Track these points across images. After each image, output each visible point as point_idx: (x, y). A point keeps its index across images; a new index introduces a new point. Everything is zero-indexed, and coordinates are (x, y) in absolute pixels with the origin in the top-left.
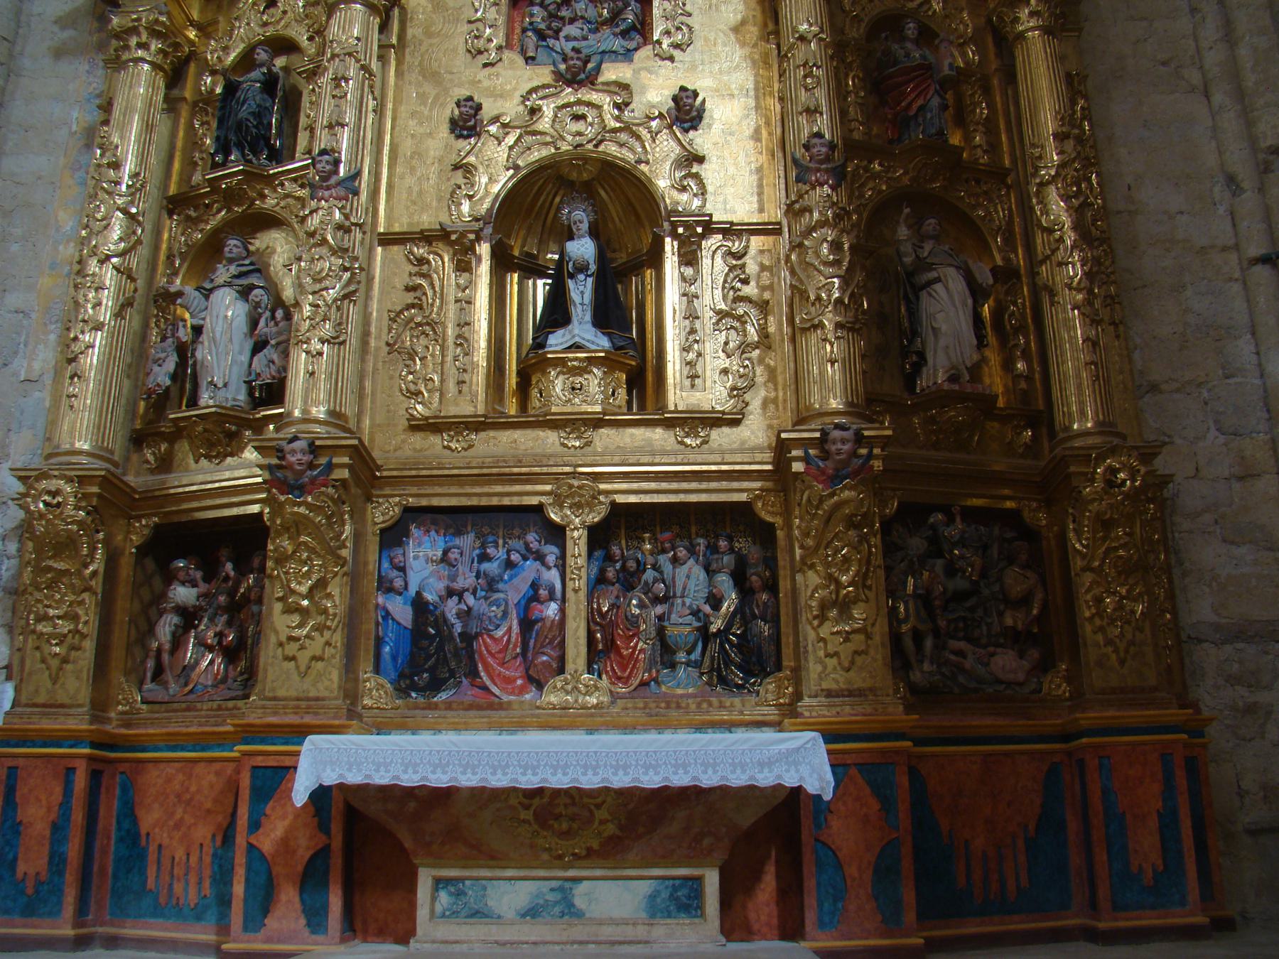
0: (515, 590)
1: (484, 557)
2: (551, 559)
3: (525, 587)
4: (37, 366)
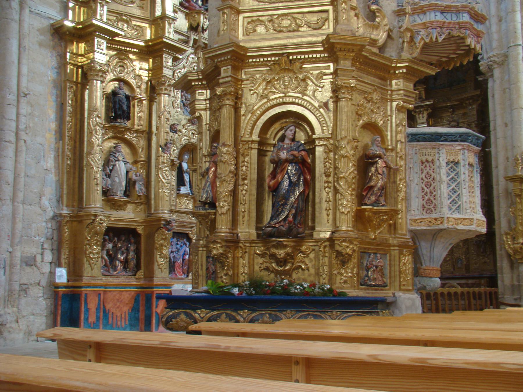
0: (181, 252)
1: (177, 244)
2: (188, 245)
3: (183, 251)
4: (49, 165)
